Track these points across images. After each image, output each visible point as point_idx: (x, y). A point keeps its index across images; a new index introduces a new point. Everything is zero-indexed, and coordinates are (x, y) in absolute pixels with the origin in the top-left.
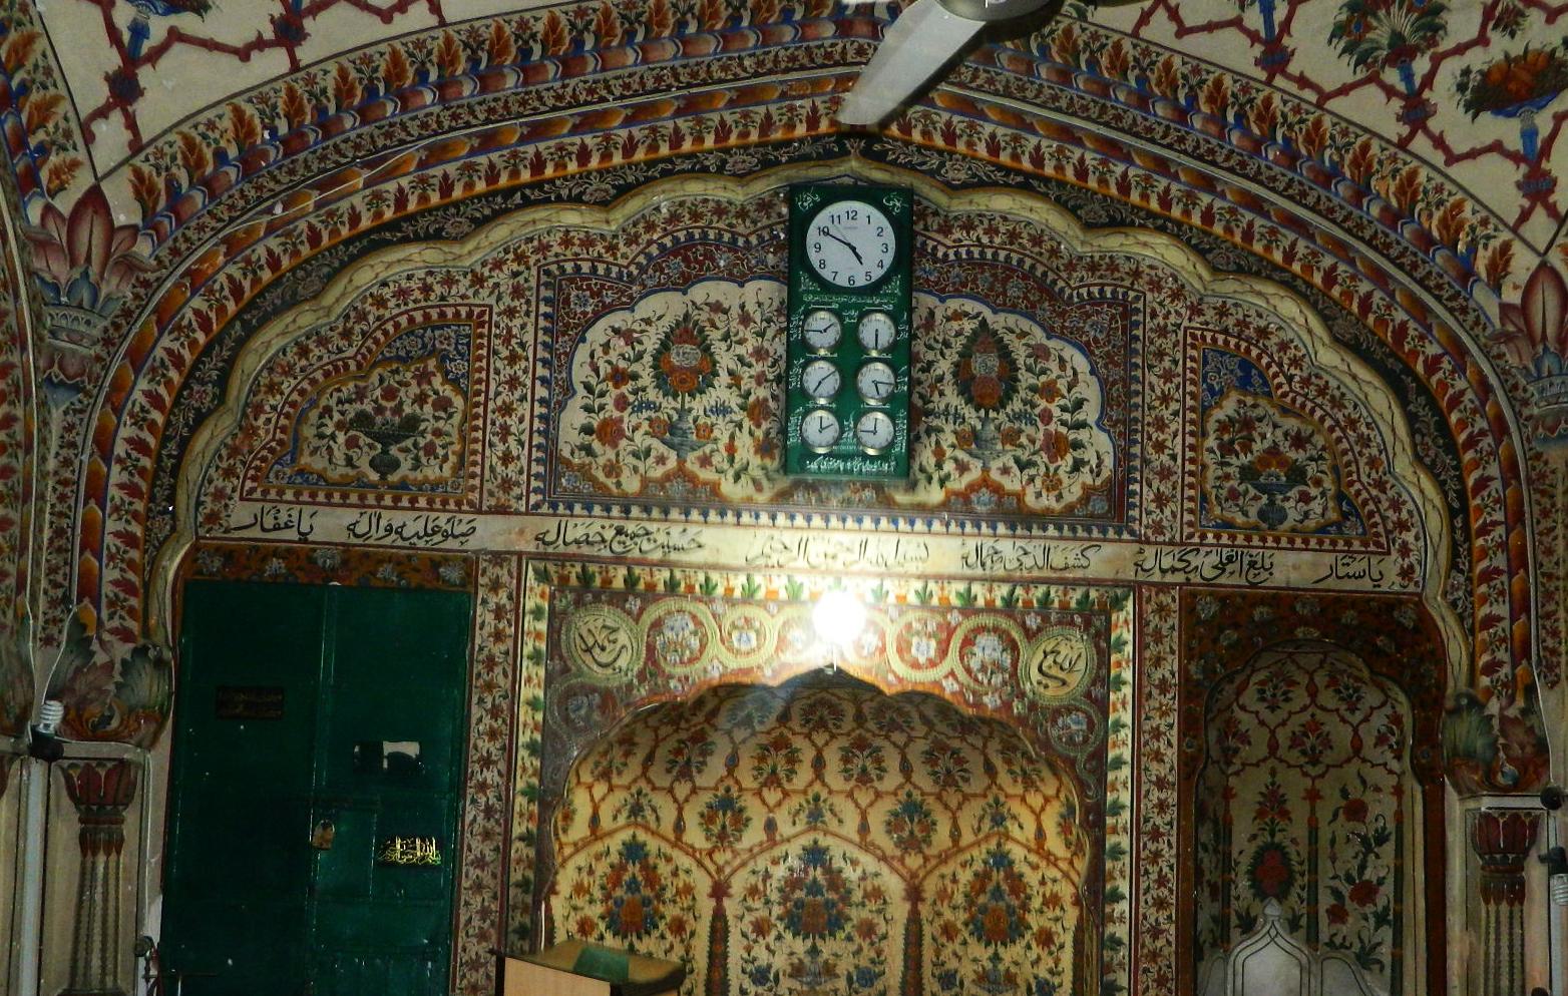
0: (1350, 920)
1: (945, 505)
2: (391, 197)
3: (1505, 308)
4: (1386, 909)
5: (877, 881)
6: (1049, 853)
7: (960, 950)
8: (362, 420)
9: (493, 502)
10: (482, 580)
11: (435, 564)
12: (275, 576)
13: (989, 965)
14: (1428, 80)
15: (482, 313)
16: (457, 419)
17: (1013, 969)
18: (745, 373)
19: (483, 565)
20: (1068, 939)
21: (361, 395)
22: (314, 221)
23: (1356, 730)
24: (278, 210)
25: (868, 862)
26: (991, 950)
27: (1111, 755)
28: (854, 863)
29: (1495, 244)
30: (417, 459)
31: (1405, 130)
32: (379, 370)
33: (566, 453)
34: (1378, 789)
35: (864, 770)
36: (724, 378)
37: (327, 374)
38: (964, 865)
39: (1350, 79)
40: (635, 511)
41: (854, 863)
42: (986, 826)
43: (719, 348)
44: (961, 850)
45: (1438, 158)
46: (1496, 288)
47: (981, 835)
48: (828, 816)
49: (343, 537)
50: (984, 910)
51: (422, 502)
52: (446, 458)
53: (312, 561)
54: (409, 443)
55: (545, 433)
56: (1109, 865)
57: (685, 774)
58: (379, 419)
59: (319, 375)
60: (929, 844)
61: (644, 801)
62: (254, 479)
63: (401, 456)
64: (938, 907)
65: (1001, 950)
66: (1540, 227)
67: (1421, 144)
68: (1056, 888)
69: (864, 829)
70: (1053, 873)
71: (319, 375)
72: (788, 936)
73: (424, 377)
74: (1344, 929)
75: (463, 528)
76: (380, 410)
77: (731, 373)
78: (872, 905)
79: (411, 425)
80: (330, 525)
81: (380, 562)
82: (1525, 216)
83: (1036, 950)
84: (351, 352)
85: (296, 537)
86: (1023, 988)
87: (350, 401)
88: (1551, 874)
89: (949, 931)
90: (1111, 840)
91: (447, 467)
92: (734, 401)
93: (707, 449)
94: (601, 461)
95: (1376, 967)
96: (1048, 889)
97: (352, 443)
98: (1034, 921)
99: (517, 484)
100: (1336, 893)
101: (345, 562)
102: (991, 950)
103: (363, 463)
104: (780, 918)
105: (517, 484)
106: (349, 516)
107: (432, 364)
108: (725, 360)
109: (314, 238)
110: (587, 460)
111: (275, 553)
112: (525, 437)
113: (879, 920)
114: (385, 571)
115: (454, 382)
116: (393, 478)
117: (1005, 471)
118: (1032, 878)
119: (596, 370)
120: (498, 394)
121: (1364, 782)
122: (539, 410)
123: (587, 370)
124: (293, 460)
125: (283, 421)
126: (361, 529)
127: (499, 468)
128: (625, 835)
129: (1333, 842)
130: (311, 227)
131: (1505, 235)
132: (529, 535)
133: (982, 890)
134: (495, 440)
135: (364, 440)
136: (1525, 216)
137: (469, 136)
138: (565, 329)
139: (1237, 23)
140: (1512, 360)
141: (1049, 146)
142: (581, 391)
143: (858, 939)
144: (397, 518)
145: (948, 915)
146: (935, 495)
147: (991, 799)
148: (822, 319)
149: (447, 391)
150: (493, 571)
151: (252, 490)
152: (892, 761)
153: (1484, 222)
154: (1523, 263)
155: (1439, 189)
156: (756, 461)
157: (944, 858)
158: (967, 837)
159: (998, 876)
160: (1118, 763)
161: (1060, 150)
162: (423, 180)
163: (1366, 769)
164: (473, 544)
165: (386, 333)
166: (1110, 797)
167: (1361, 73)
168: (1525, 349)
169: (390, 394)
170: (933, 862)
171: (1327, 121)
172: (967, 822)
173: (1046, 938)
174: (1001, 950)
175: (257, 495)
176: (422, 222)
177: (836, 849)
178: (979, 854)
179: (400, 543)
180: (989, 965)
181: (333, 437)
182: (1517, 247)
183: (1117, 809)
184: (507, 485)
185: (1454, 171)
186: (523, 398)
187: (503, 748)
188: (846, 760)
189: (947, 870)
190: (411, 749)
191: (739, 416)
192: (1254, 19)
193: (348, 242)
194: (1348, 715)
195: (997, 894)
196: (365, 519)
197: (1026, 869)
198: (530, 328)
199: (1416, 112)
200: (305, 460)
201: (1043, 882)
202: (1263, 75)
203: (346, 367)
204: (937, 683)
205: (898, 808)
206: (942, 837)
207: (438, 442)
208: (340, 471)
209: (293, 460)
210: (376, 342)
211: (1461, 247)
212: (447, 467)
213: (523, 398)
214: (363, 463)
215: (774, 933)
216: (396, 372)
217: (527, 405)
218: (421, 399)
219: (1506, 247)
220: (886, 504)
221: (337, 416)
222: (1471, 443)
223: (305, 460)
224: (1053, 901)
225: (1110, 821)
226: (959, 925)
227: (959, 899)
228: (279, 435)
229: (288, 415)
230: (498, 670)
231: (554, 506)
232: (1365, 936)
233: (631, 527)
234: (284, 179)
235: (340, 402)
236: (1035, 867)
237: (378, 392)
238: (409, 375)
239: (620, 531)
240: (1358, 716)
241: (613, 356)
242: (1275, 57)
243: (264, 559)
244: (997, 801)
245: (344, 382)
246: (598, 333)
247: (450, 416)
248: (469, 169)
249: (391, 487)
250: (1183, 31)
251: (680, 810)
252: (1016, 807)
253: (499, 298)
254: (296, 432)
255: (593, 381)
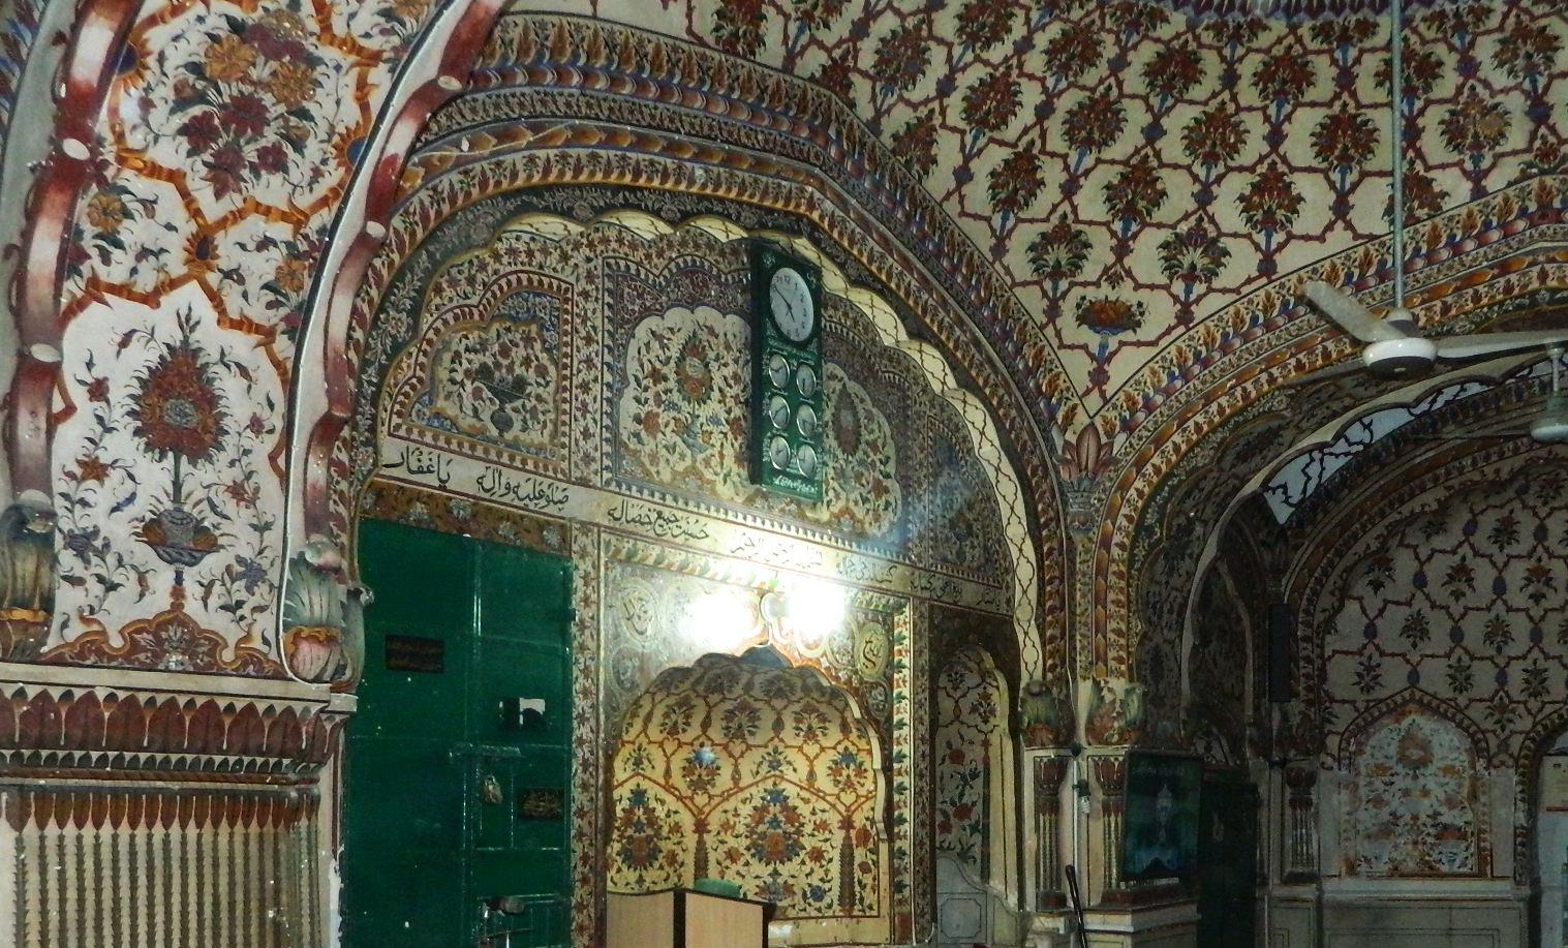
0: (954, 830)
1: (828, 524)
2: (540, 163)
3: (1067, 444)
4: (977, 822)
5: (677, 818)
6: (819, 790)
7: (743, 870)
8: (484, 373)
9: (579, 474)
10: (575, 548)
11: (542, 526)
12: (418, 521)
13: (770, 880)
14: (1064, 294)
15: (567, 290)
16: (552, 387)
17: (791, 881)
18: (729, 392)
19: (575, 533)
20: (836, 855)
21: (483, 347)
22: (486, 167)
23: (957, 705)
24: (465, 146)
25: (672, 802)
26: (770, 868)
27: (896, 718)
28: (663, 802)
29: (1070, 404)
30: (525, 421)
31: (1045, 320)
32: (496, 325)
33: (625, 438)
34: (972, 743)
35: (810, 728)
36: (716, 395)
37: (456, 318)
38: (744, 801)
39: (1029, 279)
40: (669, 500)
41: (663, 802)
42: (765, 767)
43: (714, 366)
44: (742, 790)
45: (1055, 343)
46: (1064, 431)
47: (759, 778)
48: (646, 762)
49: (473, 489)
50: (763, 836)
51: (530, 466)
52: (545, 426)
53: (450, 511)
54: (518, 403)
55: (609, 415)
56: (896, 797)
57: (673, 731)
58: (497, 375)
59: (449, 317)
60: (714, 786)
61: (644, 754)
62: (399, 414)
63: (513, 415)
64: (722, 836)
65: (780, 867)
66: (1093, 400)
67: (1050, 331)
68: (825, 816)
69: (668, 773)
70: (821, 805)
71: (449, 317)
72: (624, 868)
73: (528, 340)
74: (950, 837)
75: (558, 496)
76: (498, 365)
77: (721, 390)
78: (675, 838)
79: (520, 384)
80: (463, 475)
81: (501, 519)
82: (1088, 392)
83: (810, 864)
84: (474, 300)
85: (437, 484)
86: (800, 895)
87: (476, 352)
88: (1080, 796)
89: (732, 855)
90: (897, 780)
91: (546, 432)
92: (723, 416)
93: (709, 452)
94: (647, 449)
95: (971, 861)
96: (818, 818)
97: (477, 394)
98: (807, 842)
99: (594, 460)
100: (944, 813)
101: (474, 515)
102: (770, 868)
103: (486, 416)
104: (618, 854)
105: (594, 460)
106: (478, 468)
107: (534, 328)
108: (718, 381)
109: (484, 184)
110: (639, 447)
111: (419, 497)
112: (598, 417)
113: (678, 850)
114: (504, 528)
115: (548, 351)
116: (509, 436)
117: (856, 503)
118: (804, 810)
119: (642, 366)
120: (579, 371)
121: (962, 737)
122: (606, 394)
123: (636, 365)
124: (431, 401)
125: (422, 359)
126: (488, 484)
127: (582, 443)
128: (631, 785)
129: (942, 778)
130: (483, 172)
131: (1076, 400)
132: (604, 510)
133: (760, 821)
134: (579, 414)
135: (487, 394)
136: (1088, 392)
137: (600, 129)
138: (623, 323)
139: (988, 220)
140: (1064, 475)
141: (897, 268)
142: (633, 384)
143: (667, 868)
144: (512, 477)
145: (732, 842)
146: (825, 516)
147: (770, 750)
148: (777, 362)
149: (544, 357)
150: (582, 540)
151: (398, 427)
152: (697, 719)
153: (1068, 389)
154: (1081, 419)
155: (1052, 362)
156: (735, 468)
157: (726, 796)
158: (746, 779)
159: (774, 809)
160: (901, 725)
161: (901, 273)
162: (564, 157)
163: (964, 730)
164: (568, 510)
165: (501, 288)
166: (896, 749)
167: (1035, 278)
168: (1074, 469)
169: (505, 352)
170: (717, 800)
171: (1013, 299)
172: (747, 766)
173: (817, 855)
174: (780, 867)
175: (402, 432)
176: (560, 195)
177: (652, 791)
178: (757, 793)
179: (516, 502)
180: (770, 880)
181: (462, 385)
182: (1080, 409)
183: (901, 757)
184: (588, 459)
185: (1061, 353)
186: (595, 380)
187: (592, 707)
188: (798, 720)
189: (729, 805)
190: (539, 705)
191: (726, 428)
192: (997, 220)
193: (506, 195)
194: (951, 692)
195: (775, 822)
196: (490, 471)
197: (798, 803)
198: (599, 314)
199: (1053, 312)
200: (441, 403)
201: (813, 813)
202: (990, 257)
203: (472, 314)
204: (818, 661)
205: (837, 757)
206: (724, 781)
207: (540, 408)
208: (467, 422)
209: (431, 401)
210: (494, 295)
211: (1054, 400)
212: (546, 432)
213: (595, 380)
214: (486, 416)
215: (615, 867)
216: (508, 330)
217: (598, 386)
218: (527, 362)
219: (1075, 407)
220: (802, 516)
221: (465, 364)
222: (1046, 525)
223: (441, 403)
224: (822, 826)
225: (896, 766)
226: (742, 850)
227: (741, 829)
228: (419, 373)
229: (425, 354)
230: (587, 632)
231: (619, 485)
232: (964, 841)
233: (667, 513)
234: (469, 116)
235: (467, 350)
236: (807, 801)
237: (496, 348)
238: (518, 336)
239: (660, 515)
240: (959, 693)
241: (652, 356)
242: (999, 250)
243: (410, 502)
244: (776, 750)
245: (470, 330)
246: (642, 331)
247: (548, 383)
248: (594, 157)
249: (508, 445)
250: (963, 214)
251: (668, 762)
252: (792, 755)
253: (578, 280)
254: (433, 372)
255: (641, 376)
